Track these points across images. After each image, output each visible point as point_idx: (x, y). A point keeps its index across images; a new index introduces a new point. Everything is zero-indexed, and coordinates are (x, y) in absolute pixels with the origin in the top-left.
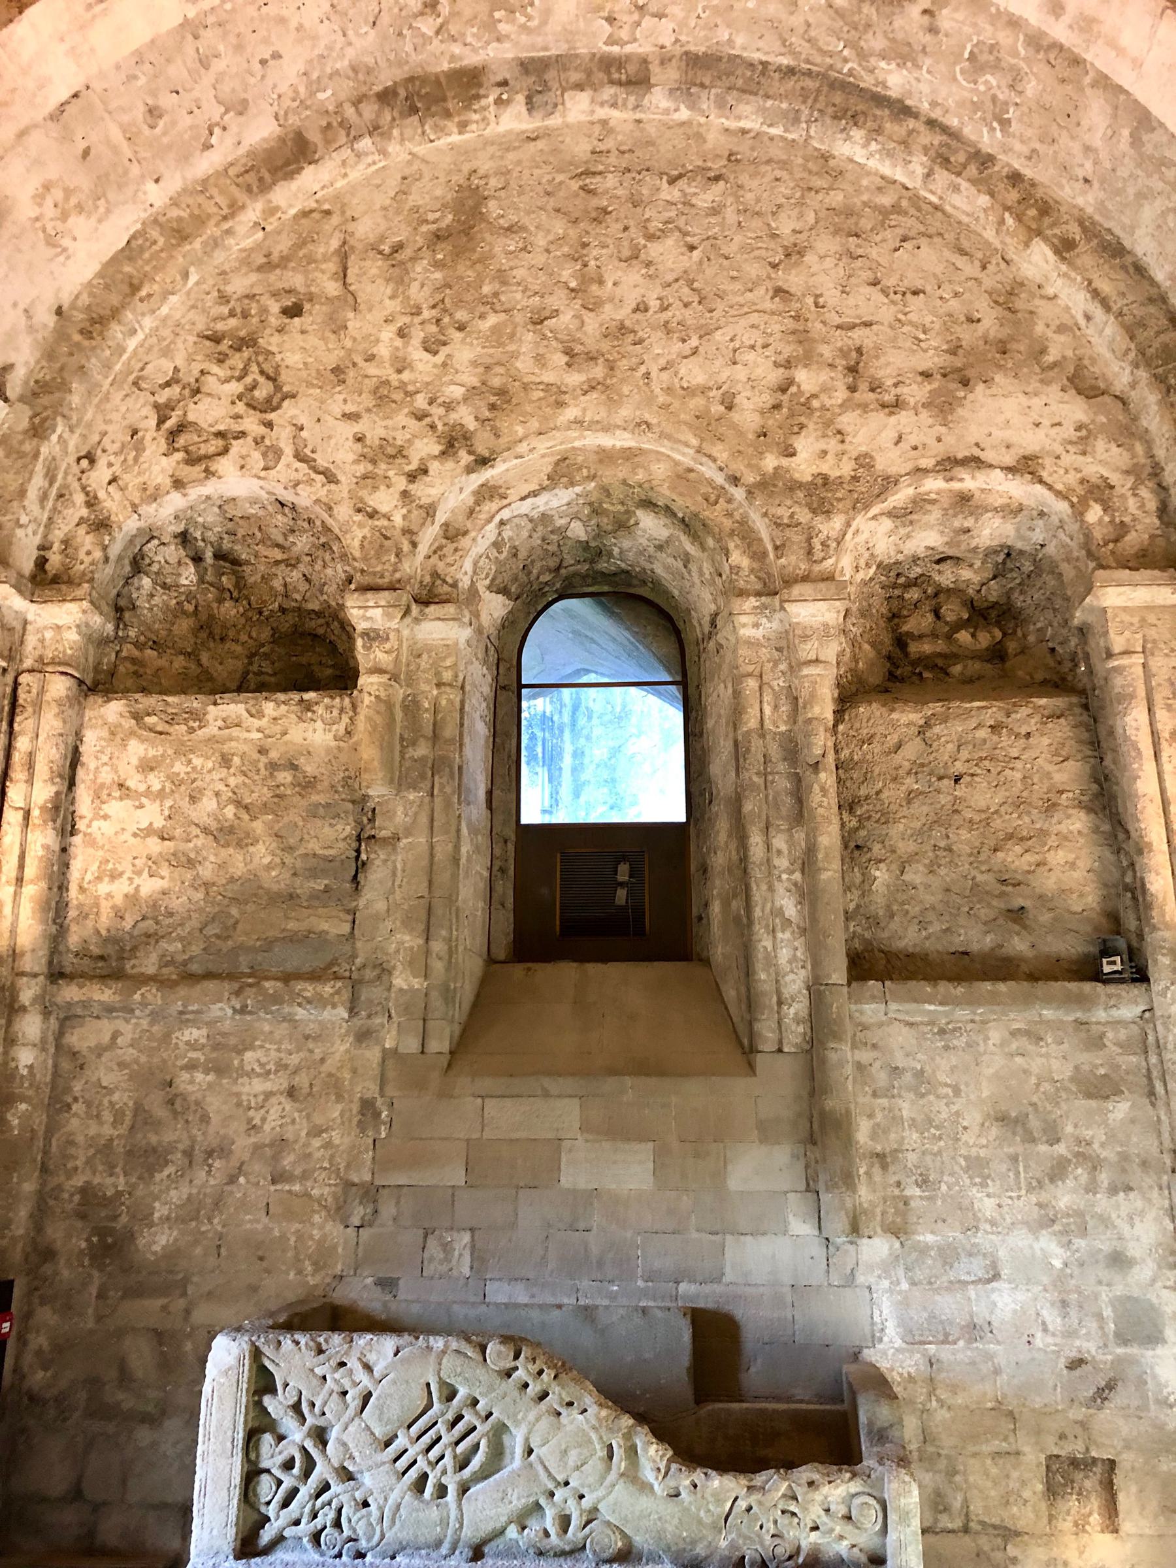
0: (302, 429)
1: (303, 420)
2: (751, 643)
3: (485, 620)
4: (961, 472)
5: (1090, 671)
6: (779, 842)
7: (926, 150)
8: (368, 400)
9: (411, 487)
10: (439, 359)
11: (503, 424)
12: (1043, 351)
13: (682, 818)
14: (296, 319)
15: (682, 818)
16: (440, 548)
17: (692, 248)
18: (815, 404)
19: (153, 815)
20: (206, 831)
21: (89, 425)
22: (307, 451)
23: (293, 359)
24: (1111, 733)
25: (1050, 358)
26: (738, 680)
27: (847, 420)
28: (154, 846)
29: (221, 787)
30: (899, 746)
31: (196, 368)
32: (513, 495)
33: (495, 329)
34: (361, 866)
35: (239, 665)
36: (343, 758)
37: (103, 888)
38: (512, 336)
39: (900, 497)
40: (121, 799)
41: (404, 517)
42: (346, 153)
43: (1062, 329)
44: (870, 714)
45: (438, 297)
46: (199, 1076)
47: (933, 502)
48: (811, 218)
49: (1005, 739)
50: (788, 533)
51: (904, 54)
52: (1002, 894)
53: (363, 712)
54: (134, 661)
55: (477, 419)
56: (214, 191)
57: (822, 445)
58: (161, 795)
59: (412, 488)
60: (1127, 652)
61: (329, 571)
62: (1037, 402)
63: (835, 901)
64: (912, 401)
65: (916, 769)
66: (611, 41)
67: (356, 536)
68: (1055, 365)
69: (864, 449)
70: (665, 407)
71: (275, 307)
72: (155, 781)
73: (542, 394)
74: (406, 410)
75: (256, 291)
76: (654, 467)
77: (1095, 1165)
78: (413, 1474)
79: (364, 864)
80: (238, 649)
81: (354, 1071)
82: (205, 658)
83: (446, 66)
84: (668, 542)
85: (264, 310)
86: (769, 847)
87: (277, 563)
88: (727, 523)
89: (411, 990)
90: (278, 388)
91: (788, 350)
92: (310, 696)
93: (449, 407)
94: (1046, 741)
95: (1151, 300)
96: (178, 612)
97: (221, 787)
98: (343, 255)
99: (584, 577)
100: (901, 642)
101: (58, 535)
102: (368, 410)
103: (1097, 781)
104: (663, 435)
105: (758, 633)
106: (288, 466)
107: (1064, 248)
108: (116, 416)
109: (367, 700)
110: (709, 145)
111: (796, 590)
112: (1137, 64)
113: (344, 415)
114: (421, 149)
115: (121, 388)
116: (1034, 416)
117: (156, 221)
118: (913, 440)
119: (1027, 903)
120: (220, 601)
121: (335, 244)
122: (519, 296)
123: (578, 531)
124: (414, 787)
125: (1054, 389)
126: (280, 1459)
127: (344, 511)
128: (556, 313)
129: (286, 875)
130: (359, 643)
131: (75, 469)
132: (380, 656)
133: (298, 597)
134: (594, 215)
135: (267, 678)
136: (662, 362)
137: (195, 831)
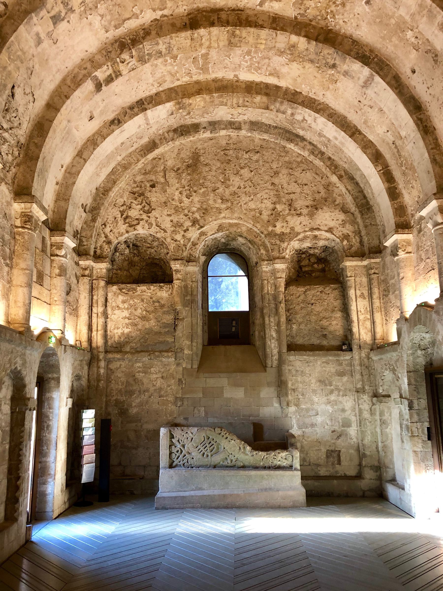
1: (157, 216)
2: (266, 272)
3: (201, 263)
4: (315, 231)
5: (343, 278)
6: (272, 320)
7: (308, 150)
8: (173, 211)
10: (190, 200)
11: (206, 218)
12: (335, 201)
13: (248, 310)
15: (248, 310)
17: (251, 171)
18: (281, 214)
19: (126, 313)
20: (139, 317)
21: (104, 216)
23: (154, 199)
24: (347, 294)
25: (337, 203)
26: (263, 280)
27: (289, 218)
28: (127, 321)
29: (142, 307)
30: (299, 296)
31: (130, 201)
32: (209, 234)
33: (204, 192)
34: (176, 326)
35: (138, 272)
36: (170, 300)
37: (116, 331)
38: (208, 195)
39: (300, 236)
42: (166, 145)
43: (339, 196)
44: (293, 289)
45: (189, 183)
46: (141, 374)
47: (309, 237)
48: (281, 164)
49: (323, 295)
50: (274, 246)
51: (303, 129)
52: (322, 331)
53: (175, 289)
54: (116, 274)
56: (133, 156)
57: (282, 224)
58: (128, 309)
60: (351, 276)
61: (162, 250)
62: (333, 214)
63: (284, 333)
65: (303, 301)
66: (231, 118)
67: (172, 246)
68: (338, 204)
70: (245, 214)
71: (148, 185)
72: (126, 305)
76: (242, 228)
77: (339, 390)
78: (202, 453)
80: (138, 268)
81: (176, 372)
82: (130, 271)
83: (190, 123)
84: (245, 244)
85: (146, 186)
86: (270, 321)
87: (149, 247)
88: (260, 243)
89: (189, 354)
90: (151, 207)
91: (275, 199)
92: (162, 284)
93: (193, 213)
94: (333, 295)
95: (360, 192)
96: (125, 260)
97: (142, 307)
98: (165, 171)
99: (223, 249)
100: (301, 267)
101: (98, 245)
103: (343, 305)
104: (245, 221)
105: (267, 270)
107: (340, 177)
108: (110, 214)
109: (176, 286)
110: (255, 143)
111: (277, 261)
112: (353, 154)
114: (183, 142)
115: (111, 206)
117: (119, 164)
118: (304, 223)
119: (327, 333)
120: (134, 257)
121: (162, 168)
123: (223, 240)
124: (187, 307)
125: (337, 210)
126: (176, 450)
127: (169, 240)
128: (218, 188)
129: (159, 328)
130: (174, 273)
131: (101, 228)
132: (179, 276)
136: (244, 202)
137: (136, 317)
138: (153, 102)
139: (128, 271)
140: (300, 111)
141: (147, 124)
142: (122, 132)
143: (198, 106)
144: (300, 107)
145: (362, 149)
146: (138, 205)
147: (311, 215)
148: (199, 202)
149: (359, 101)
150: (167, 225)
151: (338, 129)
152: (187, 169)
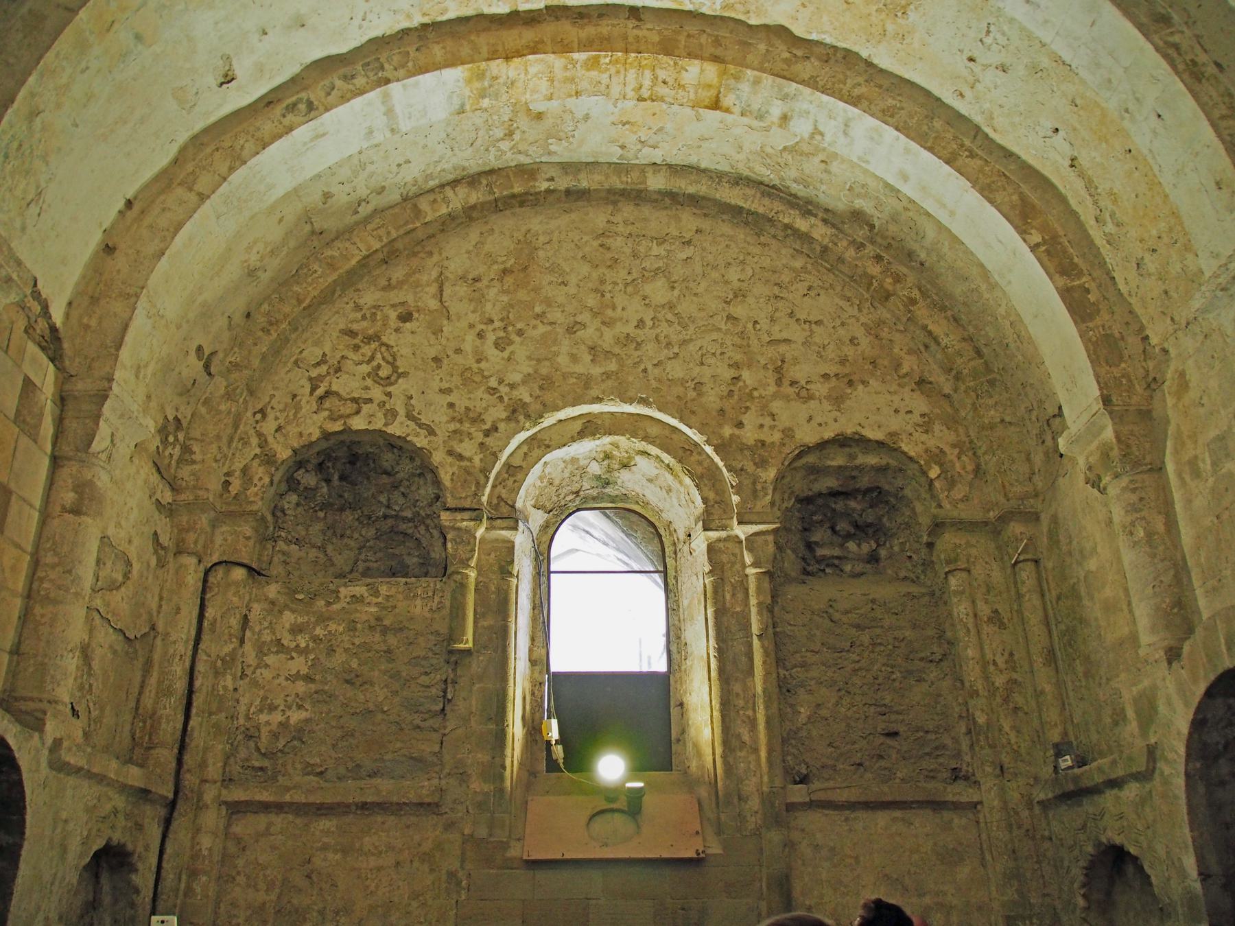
0: (411, 398)
1: (412, 392)
8: (457, 380)
10: (506, 354)
14: (408, 324)
16: (504, 480)
18: (756, 394)
22: (415, 413)
25: (905, 369)
33: (543, 336)
37: (263, 718)
40: (277, 652)
41: (481, 460)
46: (330, 856)
54: (284, 553)
55: (531, 395)
57: (761, 420)
58: (304, 652)
59: (488, 441)
61: (422, 492)
62: (896, 398)
64: (817, 394)
69: (787, 424)
71: (393, 315)
74: (483, 388)
75: (380, 303)
79: (449, 701)
80: (352, 544)
82: (330, 548)
85: (386, 318)
93: (512, 386)
102: (457, 387)
106: (402, 423)
113: (440, 390)
116: (895, 406)
118: (819, 419)
121: (434, 274)
128: (584, 326)
133: (397, 508)
134: (609, 263)
135: (371, 564)
138: (410, 64)
140: (805, 106)
141: (392, 130)
142: (318, 137)
143: (534, 91)
144: (807, 91)
145: (981, 191)
146: (360, 363)
147: (837, 400)
148: (529, 358)
149: (971, 60)
150: (438, 416)
151: (914, 146)
152: (501, 280)
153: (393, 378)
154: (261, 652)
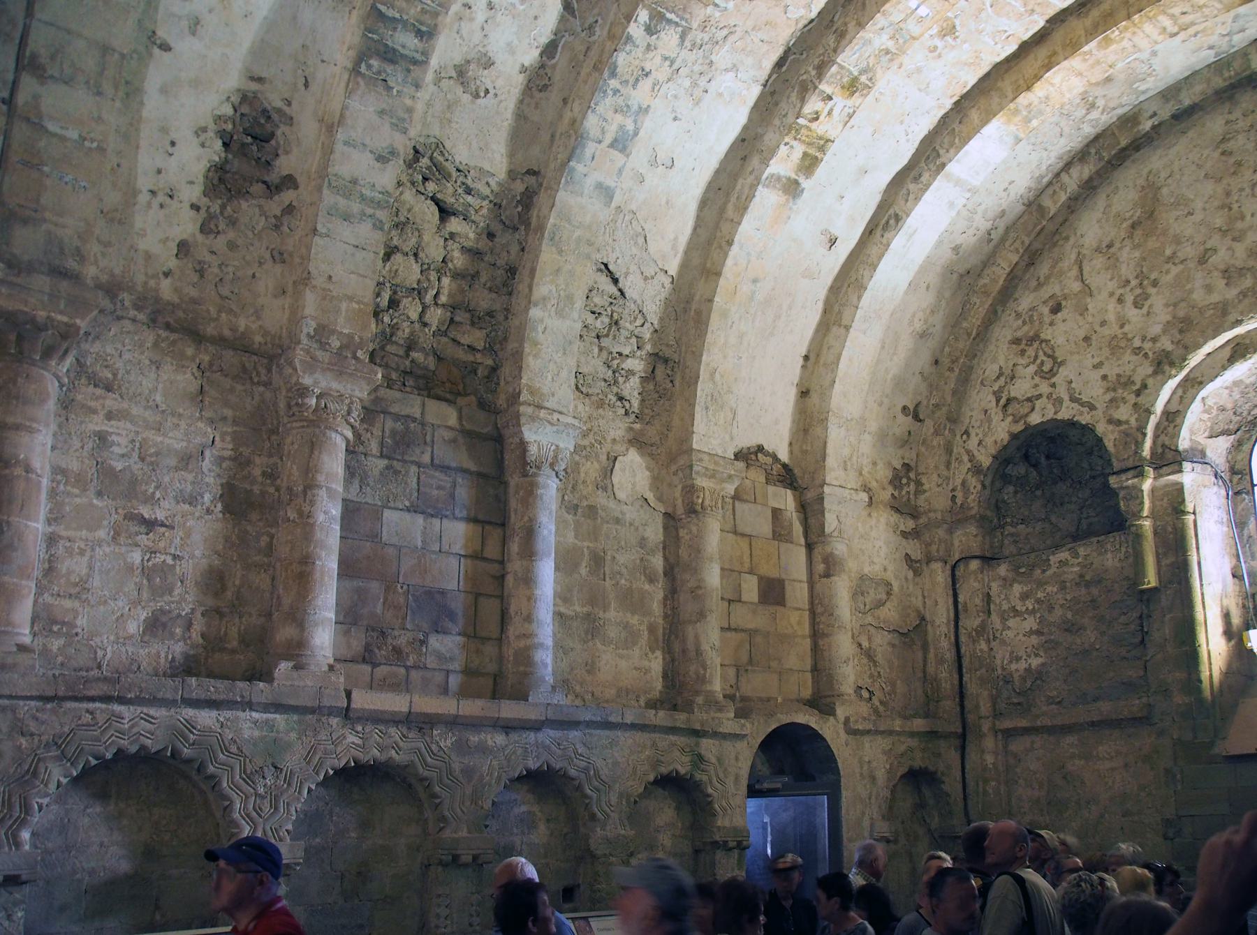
0: (1071, 382)
1: (1072, 377)
9: (1140, 399)
19: (1031, 623)
23: (1060, 340)
28: (1034, 640)
37: (1014, 667)
40: (1014, 616)
41: (1137, 420)
58: (1033, 612)
59: (1141, 400)
71: (1046, 310)
72: (1030, 604)
73: (1212, 311)
74: (1129, 351)
93: (1154, 340)
102: (1107, 358)
106: (1068, 407)
121: (1073, 256)
122: (1189, 249)
134: (1232, 170)
139: (1046, 519)
148: (1167, 305)
150: (1095, 391)
152: (1131, 236)
153: (1055, 369)
154: (1004, 619)
